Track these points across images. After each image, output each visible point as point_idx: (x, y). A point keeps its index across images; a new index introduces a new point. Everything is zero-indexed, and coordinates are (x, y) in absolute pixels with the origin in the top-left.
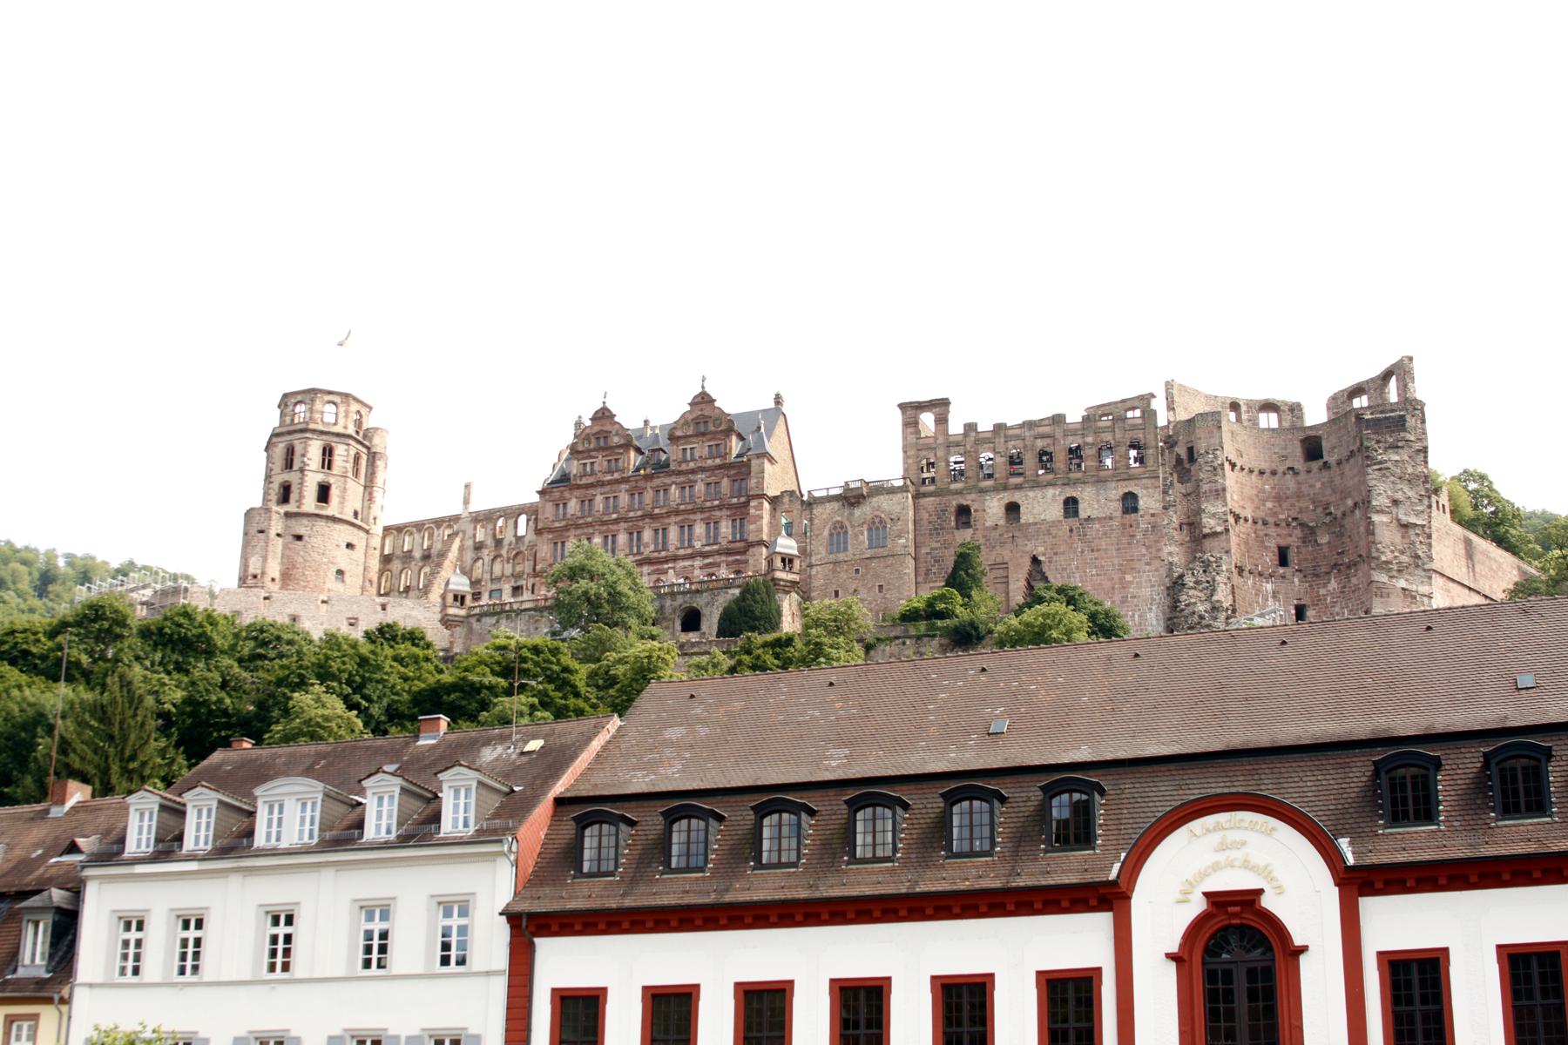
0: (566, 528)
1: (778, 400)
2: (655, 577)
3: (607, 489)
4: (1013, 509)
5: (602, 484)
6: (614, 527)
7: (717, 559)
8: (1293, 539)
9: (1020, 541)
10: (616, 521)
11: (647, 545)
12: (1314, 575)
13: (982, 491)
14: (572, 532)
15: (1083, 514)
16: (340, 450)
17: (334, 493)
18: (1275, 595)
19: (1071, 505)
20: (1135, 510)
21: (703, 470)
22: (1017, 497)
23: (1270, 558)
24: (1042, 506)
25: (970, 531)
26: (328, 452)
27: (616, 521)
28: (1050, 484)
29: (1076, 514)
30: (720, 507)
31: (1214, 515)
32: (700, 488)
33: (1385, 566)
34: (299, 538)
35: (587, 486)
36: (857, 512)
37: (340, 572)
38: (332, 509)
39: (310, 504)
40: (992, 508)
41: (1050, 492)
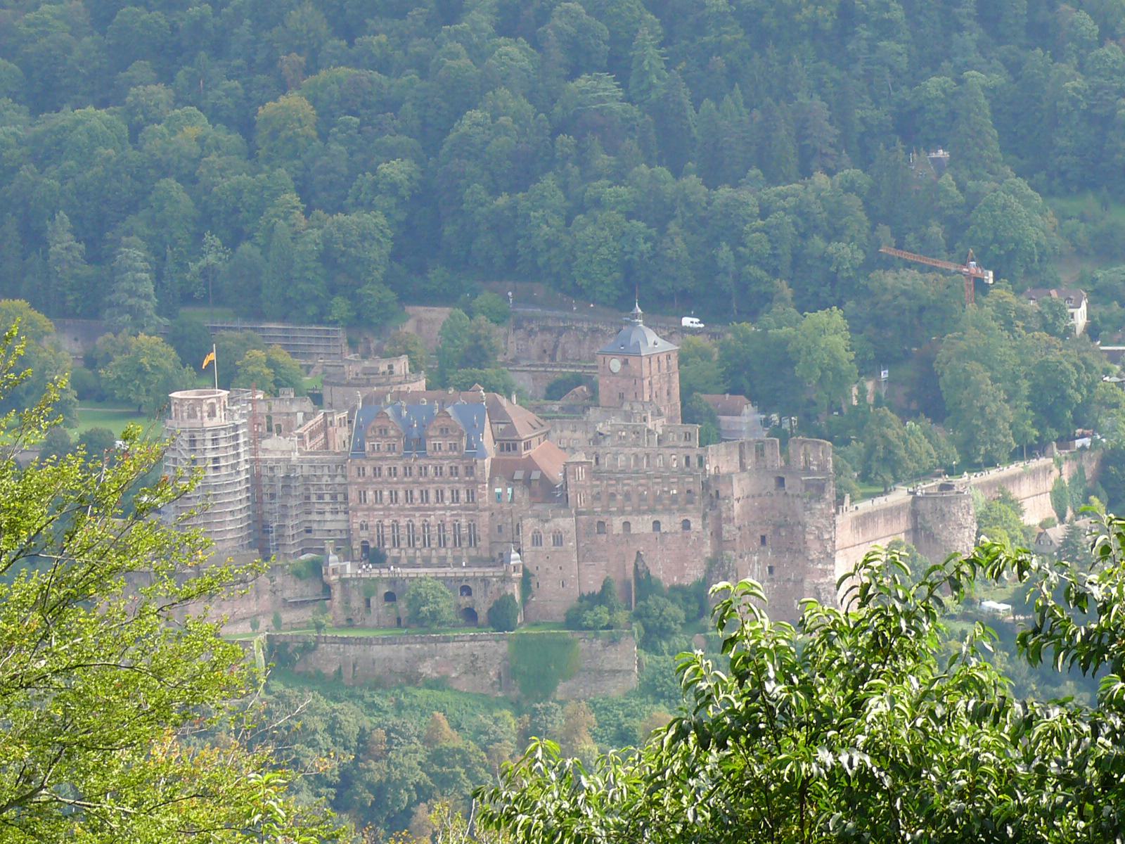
0: (365, 483)
2: (422, 518)
3: (389, 462)
4: (627, 525)
5: (386, 459)
6: (396, 486)
7: (460, 512)
8: (768, 532)
9: (631, 543)
10: (396, 483)
11: (417, 500)
12: (778, 551)
13: (611, 513)
14: (370, 486)
15: (663, 530)
18: (758, 562)
19: (657, 525)
20: (689, 528)
21: (448, 458)
22: (629, 519)
23: (756, 543)
25: (604, 537)
27: (396, 483)
28: (644, 513)
29: (659, 530)
30: (459, 482)
31: (728, 532)
32: (446, 469)
33: (812, 561)
36: (547, 525)
40: (617, 524)
41: (646, 517)
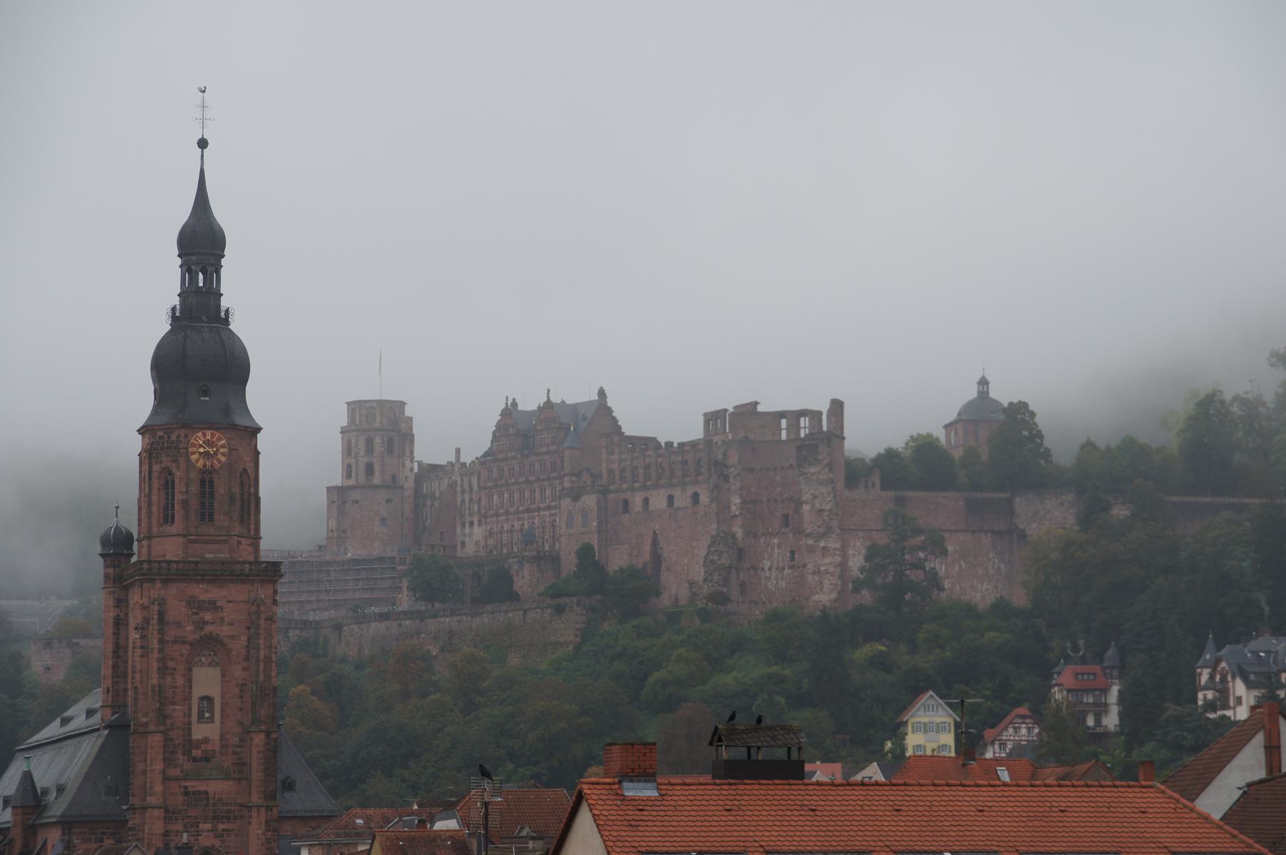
1: (602, 393)
4: (646, 500)
13: (633, 490)
16: (378, 440)
17: (377, 467)
18: (779, 545)
19: (671, 498)
24: (658, 501)
26: (369, 443)
34: (357, 502)
35: (501, 460)
37: (383, 520)
38: (377, 480)
39: (362, 479)
40: (637, 500)
41: (662, 491)
